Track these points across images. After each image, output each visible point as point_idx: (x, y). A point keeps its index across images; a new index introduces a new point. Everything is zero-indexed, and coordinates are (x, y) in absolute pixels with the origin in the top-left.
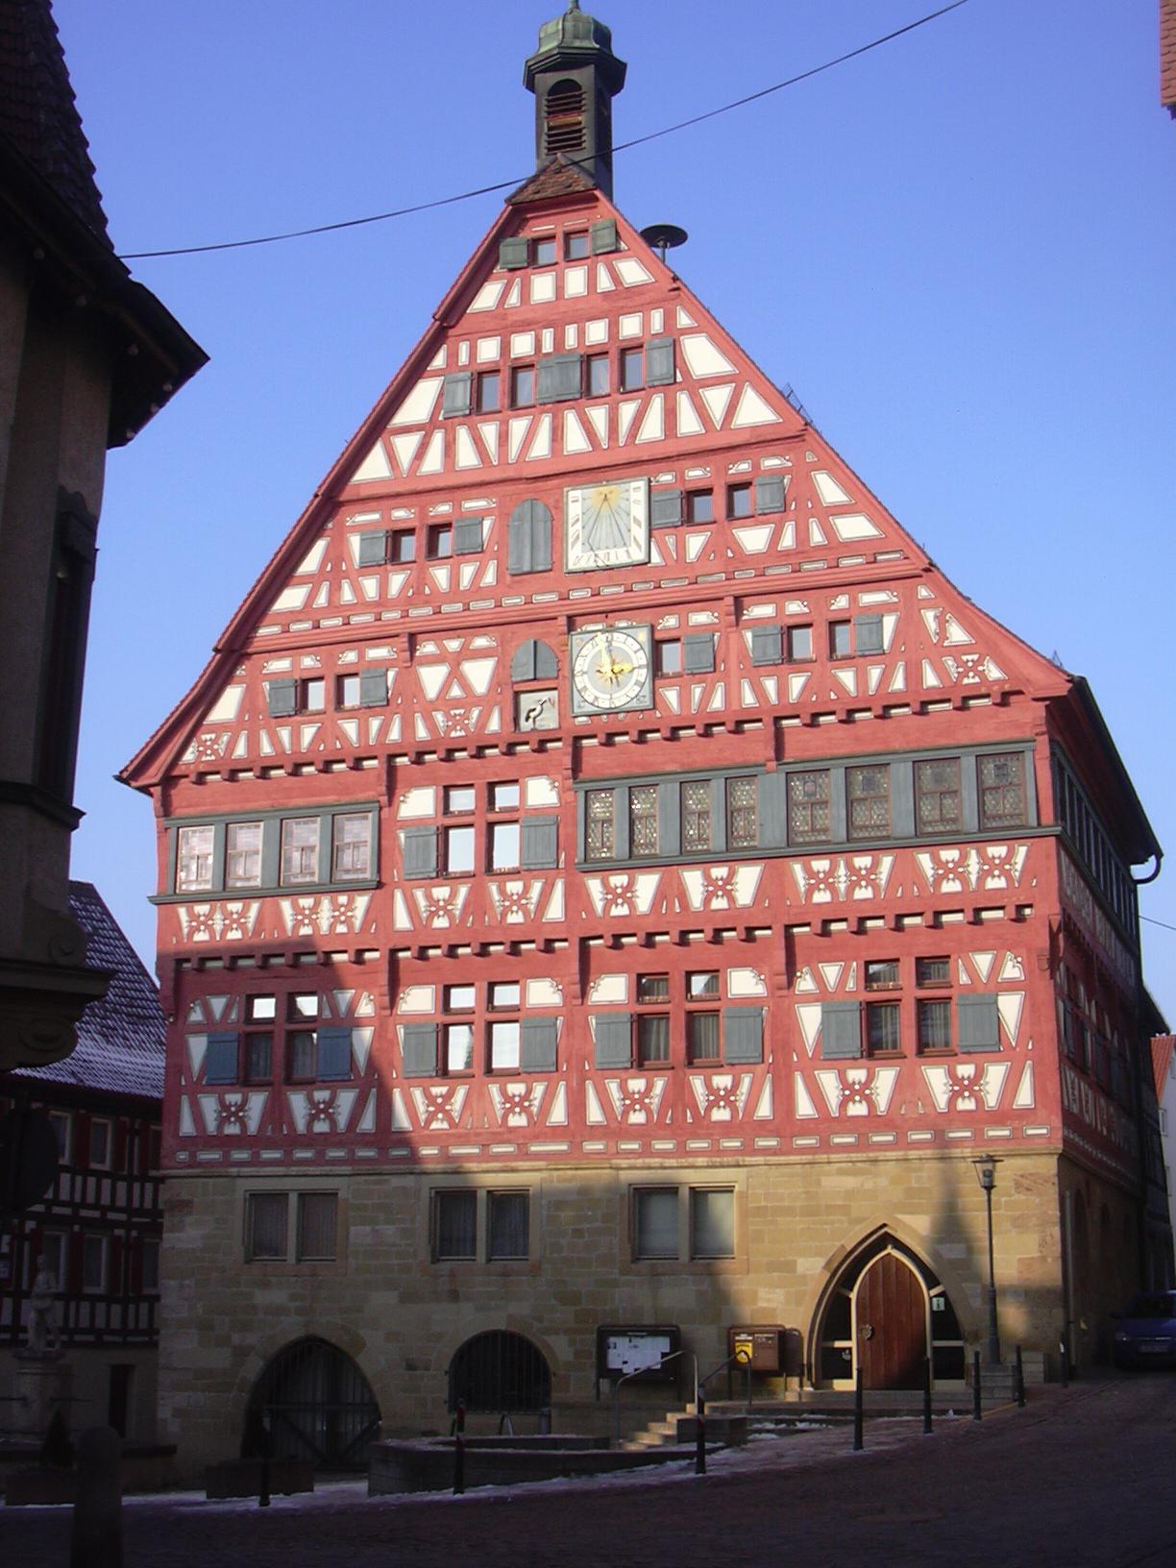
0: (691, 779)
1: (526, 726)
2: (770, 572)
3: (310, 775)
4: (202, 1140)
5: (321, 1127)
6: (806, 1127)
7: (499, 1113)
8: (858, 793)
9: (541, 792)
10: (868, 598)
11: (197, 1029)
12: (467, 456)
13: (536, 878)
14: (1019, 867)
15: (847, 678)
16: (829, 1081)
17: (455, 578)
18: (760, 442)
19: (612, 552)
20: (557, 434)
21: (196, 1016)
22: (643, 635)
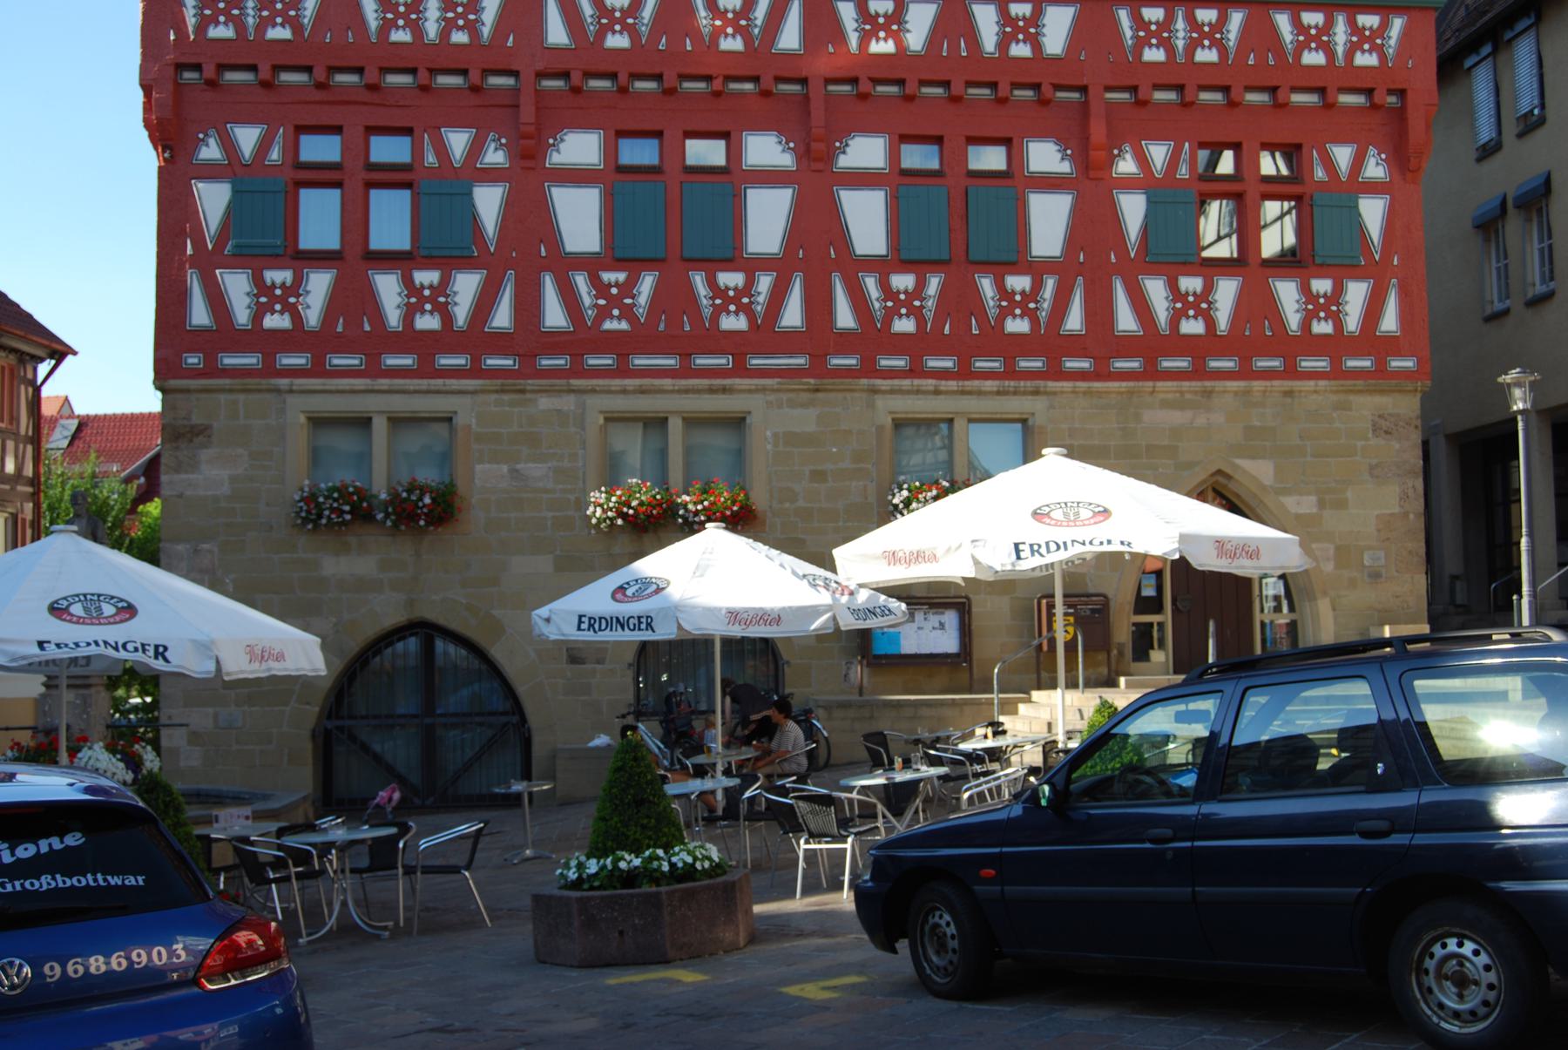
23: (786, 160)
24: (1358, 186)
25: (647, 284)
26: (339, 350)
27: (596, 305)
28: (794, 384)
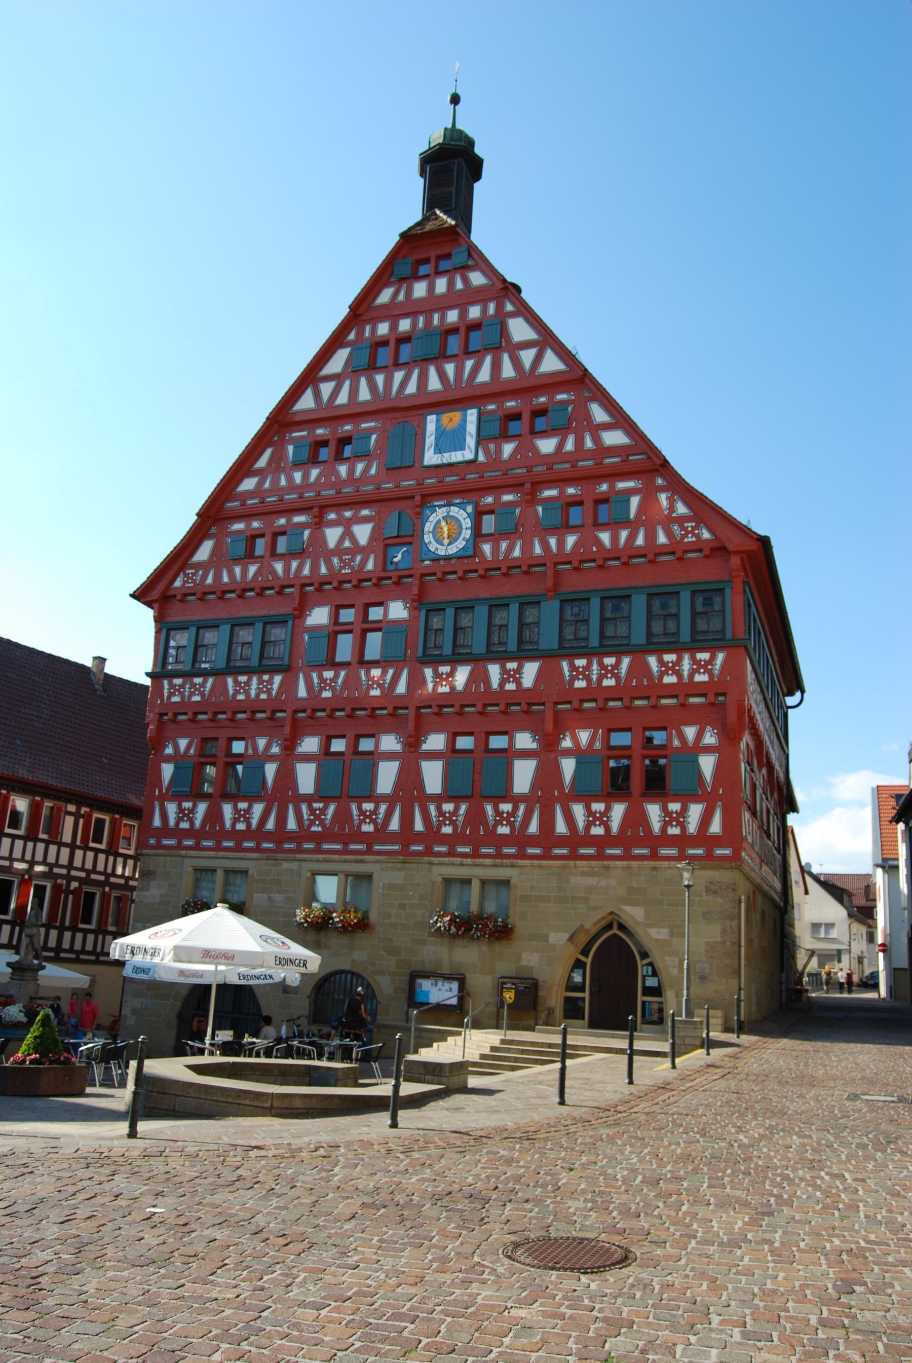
0: (496, 606)
1: (391, 567)
2: (556, 467)
3: (250, 597)
4: (165, 831)
5: (241, 826)
6: (561, 841)
7: (356, 822)
8: (608, 615)
9: (398, 610)
10: (621, 485)
11: (168, 759)
12: (364, 395)
13: (391, 666)
14: (717, 667)
15: (605, 537)
16: (578, 810)
17: (351, 471)
18: (553, 383)
19: (453, 454)
20: (423, 380)
21: (169, 750)
22: (470, 509)
23: (398, 747)
24: (699, 748)
25: (332, 808)
26: (206, 839)
27: (309, 819)
28: (392, 859)
